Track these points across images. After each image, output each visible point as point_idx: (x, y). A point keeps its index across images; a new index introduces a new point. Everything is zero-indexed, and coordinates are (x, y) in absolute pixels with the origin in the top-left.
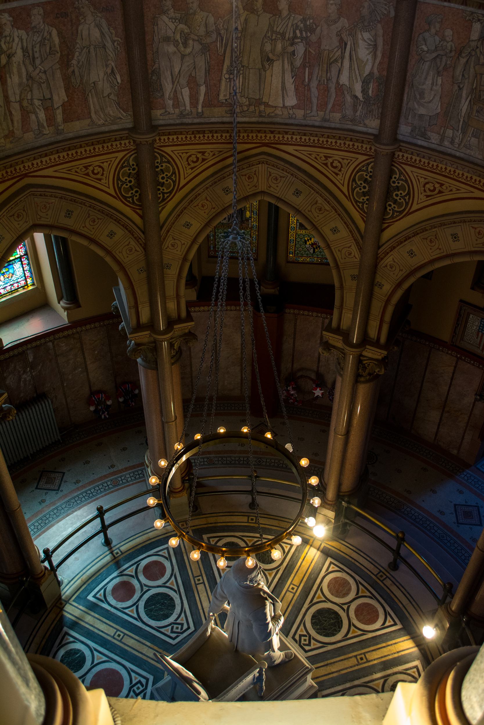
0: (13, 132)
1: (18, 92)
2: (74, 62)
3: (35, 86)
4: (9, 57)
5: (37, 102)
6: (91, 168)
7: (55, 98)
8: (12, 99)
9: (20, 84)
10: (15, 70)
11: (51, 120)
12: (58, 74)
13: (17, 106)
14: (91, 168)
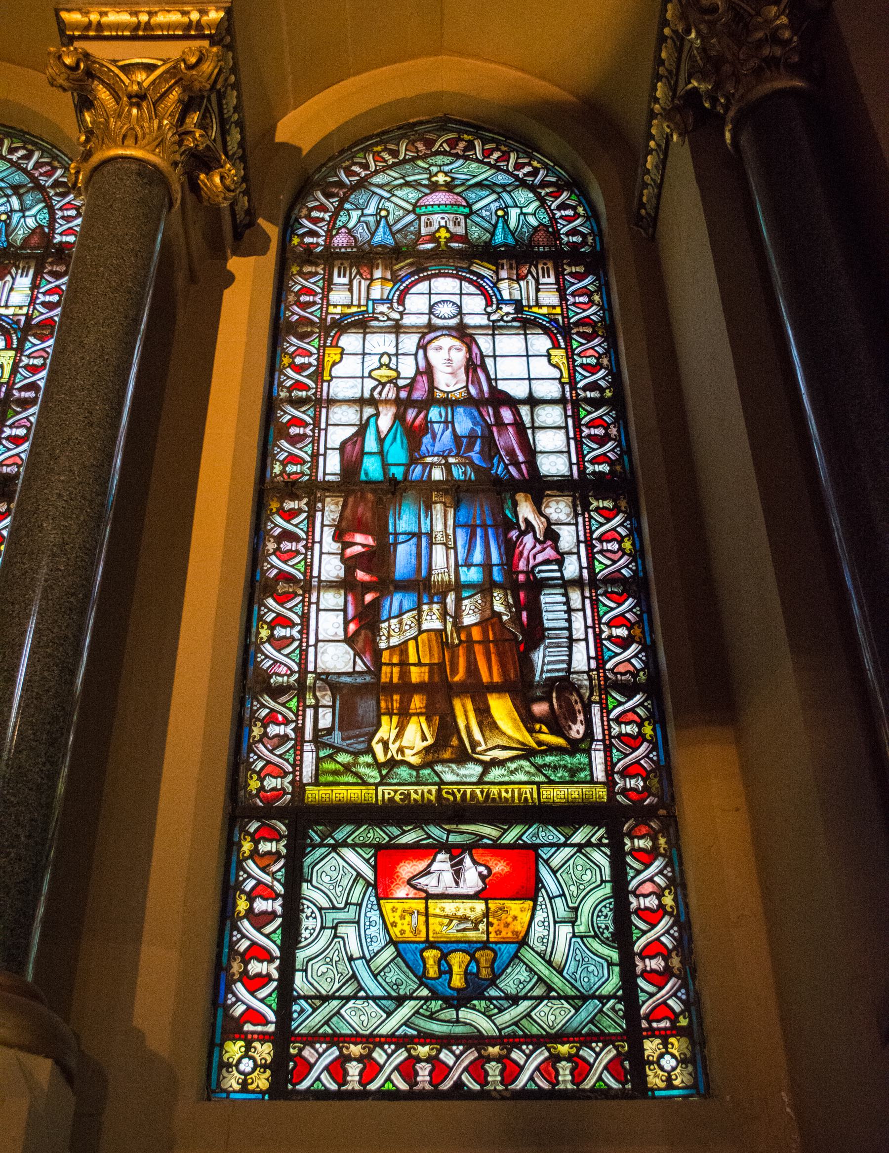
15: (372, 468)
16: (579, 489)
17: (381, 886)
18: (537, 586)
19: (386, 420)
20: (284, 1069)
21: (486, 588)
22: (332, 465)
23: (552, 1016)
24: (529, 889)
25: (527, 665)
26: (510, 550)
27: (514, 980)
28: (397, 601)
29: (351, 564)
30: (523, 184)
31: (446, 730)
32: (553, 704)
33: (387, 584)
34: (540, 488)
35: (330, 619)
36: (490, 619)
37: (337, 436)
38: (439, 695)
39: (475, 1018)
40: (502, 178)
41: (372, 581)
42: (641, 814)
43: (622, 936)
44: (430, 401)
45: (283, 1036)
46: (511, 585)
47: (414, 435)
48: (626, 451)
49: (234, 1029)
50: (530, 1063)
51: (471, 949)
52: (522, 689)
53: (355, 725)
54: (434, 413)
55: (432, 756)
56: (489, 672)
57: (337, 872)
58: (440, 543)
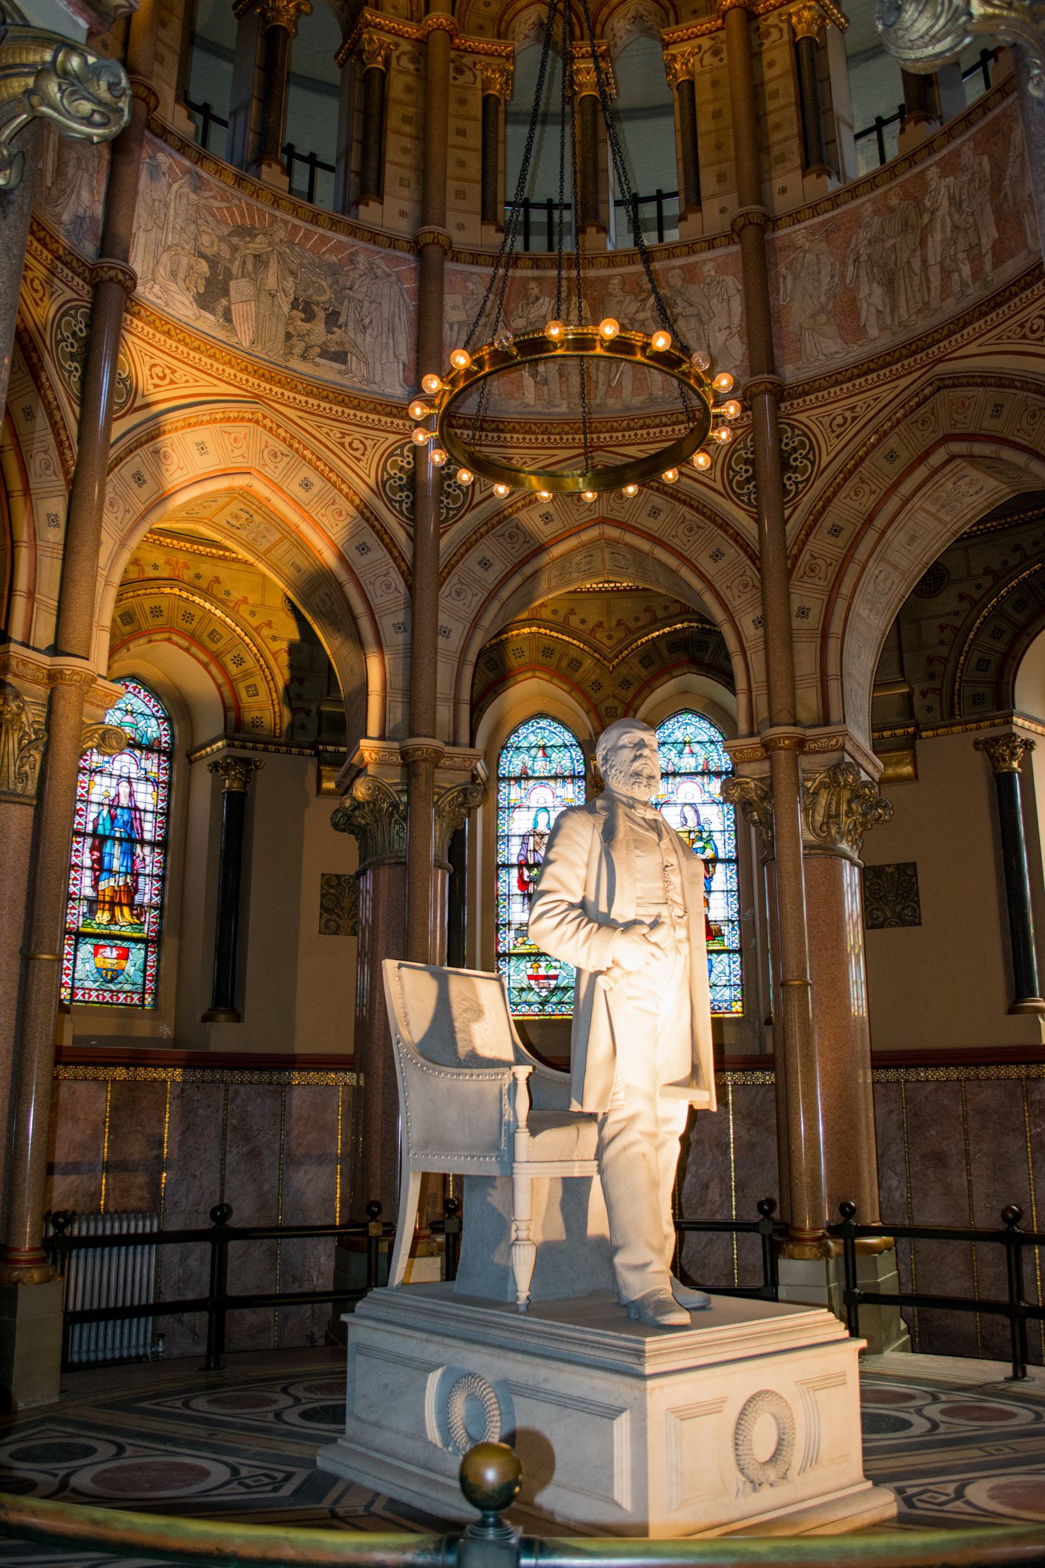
0: (928, 303)
1: (939, 251)
2: (1006, 182)
3: (961, 236)
4: (933, 213)
5: (961, 256)
6: (1028, 325)
7: (984, 240)
8: (932, 262)
9: (942, 241)
10: (938, 226)
11: (977, 273)
12: (989, 208)
13: (937, 269)
14: (1028, 325)
15: (100, 830)
16: (153, 844)
17: (95, 954)
18: (138, 875)
19: (105, 813)
20: (73, 995)
21: (126, 874)
22: (90, 828)
23: (127, 987)
24: (126, 958)
25: (133, 899)
26: (133, 862)
27: (121, 978)
28: (105, 875)
29: (94, 861)
30: (154, 716)
31: (113, 916)
32: (138, 910)
33: (102, 870)
34: (143, 842)
35: (87, 881)
36: (126, 884)
37: (92, 816)
38: (112, 904)
39: (111, 986)
40: (148, 712)
41: (100, 868)
42: (153, 942)
43: (144, 971)
44: (118, 806)
45: (72, 988)
46: (132, 874)
47: (113, 818)
48: (167, 833)
49: (62, 985)
50: (122, 996)
51: (113, 971)
52: (131, 905)
53: (92, 912)
54: (119, 811)
55: (110, 922)
56: (124, 901)
57: (86, 949)
58: (116, 858)
